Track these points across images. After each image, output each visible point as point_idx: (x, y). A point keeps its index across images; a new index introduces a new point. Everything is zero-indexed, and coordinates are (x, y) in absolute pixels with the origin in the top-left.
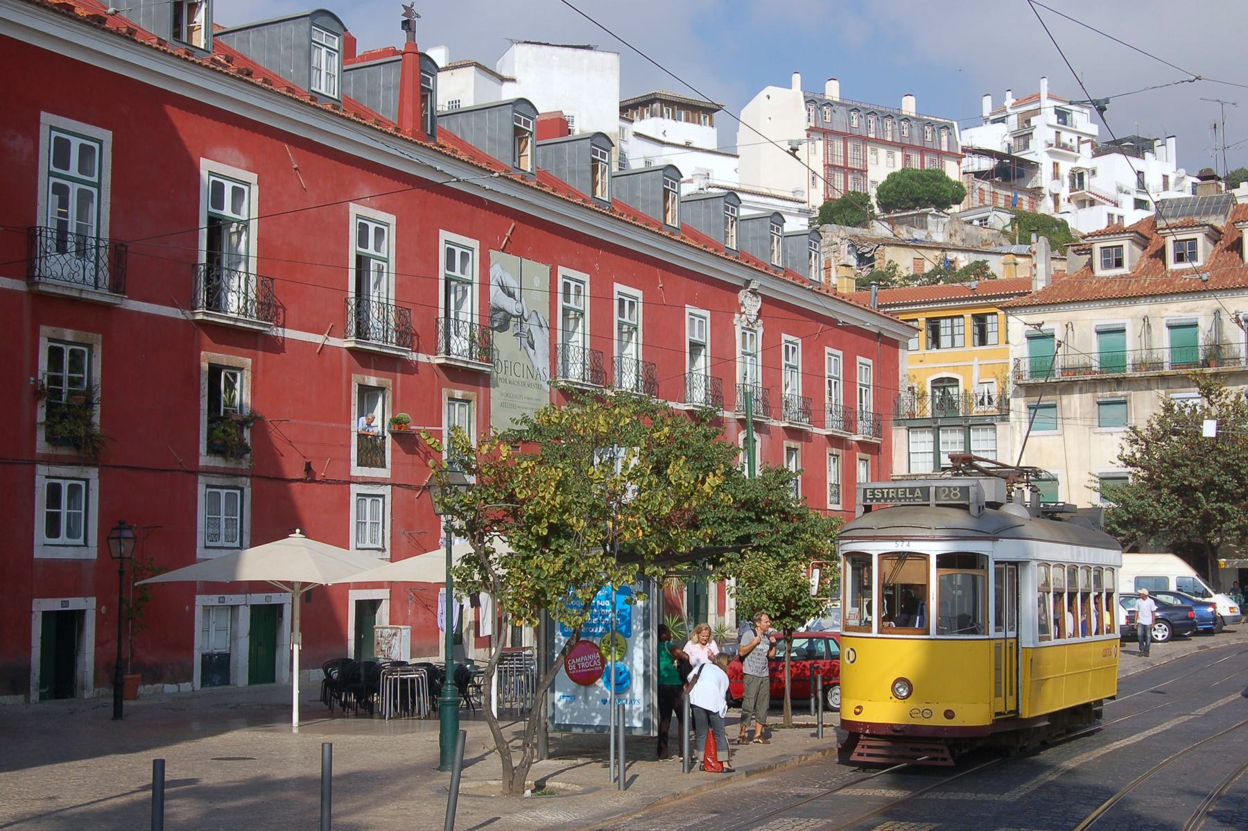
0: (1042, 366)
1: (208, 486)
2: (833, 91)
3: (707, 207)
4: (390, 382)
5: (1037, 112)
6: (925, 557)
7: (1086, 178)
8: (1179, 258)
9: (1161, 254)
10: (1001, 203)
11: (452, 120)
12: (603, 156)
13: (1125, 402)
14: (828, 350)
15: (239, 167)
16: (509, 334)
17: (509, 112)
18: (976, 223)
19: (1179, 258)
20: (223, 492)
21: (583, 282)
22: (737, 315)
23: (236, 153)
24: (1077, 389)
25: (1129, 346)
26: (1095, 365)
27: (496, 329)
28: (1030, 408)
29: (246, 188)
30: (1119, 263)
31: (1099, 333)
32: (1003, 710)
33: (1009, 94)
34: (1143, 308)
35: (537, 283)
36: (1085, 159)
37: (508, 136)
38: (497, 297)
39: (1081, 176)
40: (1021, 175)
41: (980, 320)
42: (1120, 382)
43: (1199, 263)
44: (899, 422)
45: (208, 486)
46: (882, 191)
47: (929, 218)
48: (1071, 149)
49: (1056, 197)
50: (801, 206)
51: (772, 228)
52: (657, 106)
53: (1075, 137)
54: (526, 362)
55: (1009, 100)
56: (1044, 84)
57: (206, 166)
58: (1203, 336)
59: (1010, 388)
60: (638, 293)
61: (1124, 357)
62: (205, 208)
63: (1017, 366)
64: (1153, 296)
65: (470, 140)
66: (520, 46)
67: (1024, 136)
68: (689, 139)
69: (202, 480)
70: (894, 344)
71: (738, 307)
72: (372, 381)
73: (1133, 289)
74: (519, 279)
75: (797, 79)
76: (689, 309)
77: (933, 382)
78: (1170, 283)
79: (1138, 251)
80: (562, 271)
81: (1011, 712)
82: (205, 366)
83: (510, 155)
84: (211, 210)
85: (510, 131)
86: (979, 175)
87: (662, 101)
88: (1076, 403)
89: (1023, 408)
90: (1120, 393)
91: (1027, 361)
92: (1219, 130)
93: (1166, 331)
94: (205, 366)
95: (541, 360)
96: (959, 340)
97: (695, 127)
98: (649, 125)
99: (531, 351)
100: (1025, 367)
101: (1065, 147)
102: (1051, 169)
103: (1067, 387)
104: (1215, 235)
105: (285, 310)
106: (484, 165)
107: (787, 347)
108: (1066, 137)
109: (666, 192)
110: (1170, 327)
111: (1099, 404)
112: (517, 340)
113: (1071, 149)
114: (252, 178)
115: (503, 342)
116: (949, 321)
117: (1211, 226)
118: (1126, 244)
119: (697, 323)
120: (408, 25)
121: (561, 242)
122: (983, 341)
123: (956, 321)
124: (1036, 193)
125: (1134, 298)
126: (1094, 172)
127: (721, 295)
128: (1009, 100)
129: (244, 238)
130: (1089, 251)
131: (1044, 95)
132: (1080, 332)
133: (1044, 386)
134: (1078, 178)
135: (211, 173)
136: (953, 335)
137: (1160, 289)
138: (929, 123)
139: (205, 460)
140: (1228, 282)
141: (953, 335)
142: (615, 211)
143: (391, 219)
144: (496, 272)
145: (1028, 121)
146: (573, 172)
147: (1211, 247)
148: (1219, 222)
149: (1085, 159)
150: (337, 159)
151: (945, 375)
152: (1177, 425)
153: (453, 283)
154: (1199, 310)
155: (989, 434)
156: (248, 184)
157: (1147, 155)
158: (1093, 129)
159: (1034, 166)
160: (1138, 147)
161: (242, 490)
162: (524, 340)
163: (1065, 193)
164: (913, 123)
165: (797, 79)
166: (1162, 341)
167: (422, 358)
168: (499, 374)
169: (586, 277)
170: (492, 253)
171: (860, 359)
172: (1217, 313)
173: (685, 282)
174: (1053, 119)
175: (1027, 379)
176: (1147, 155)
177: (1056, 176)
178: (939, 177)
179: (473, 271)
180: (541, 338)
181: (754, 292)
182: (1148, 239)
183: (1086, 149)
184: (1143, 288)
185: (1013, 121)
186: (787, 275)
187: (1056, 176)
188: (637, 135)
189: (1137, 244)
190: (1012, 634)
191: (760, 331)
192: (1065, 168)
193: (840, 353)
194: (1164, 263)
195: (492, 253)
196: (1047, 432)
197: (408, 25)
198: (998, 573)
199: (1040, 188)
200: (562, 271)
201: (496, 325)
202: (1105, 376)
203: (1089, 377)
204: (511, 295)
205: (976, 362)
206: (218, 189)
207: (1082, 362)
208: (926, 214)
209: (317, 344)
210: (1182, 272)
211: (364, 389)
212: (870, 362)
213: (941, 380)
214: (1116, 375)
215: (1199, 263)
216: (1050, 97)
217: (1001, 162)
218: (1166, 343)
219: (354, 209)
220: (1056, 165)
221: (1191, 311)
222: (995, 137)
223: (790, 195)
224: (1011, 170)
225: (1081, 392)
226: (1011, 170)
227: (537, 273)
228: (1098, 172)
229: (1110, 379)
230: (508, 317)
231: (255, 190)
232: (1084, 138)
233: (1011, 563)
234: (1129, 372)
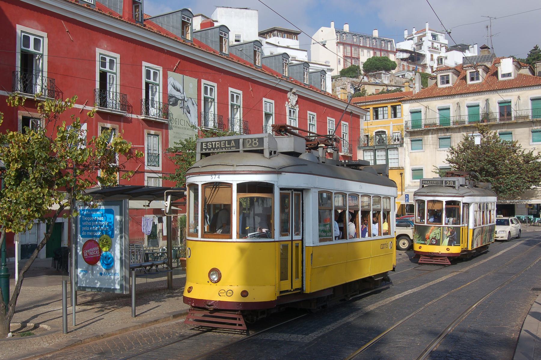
0: (416, 123)
2: (346, 28)
3: (275, 59)
4: (118, 126)
5: (424, 35)
6: (229, 185)
7: (443, 60)
8: (472, 79)
9: (465, 78)
11: (157, 19)
12: (225, 35)
13: (450, 138)
14: (328, 118)
15: (37, 29)
16: (177, 107)
17: (179, 14)
18: (401, 76)
19: (472, 79)
22: (287, 102)
23: (36, 23)
24: (430, 133)
25: (451, 115)
26: (438, 122)
27: (171, 105)
28: (412, 141)
29: (41, 39)
30: (448, 82)
31: (439, 110)
32: (289, 288)
33: (414, 29)
34: (457, 99)
35: (191, 85)
36: (443, 53)
37: (179, 25)
38: (171, 90)
39: (441, 59)
40: (419, 59)
41: (394, 108)
42: (448, 130)
43: (480, 81)
44: (360, 148)
46: (365, 65)
47: (382, 75)
48: (438, 49)
50: (328, 67)
51: (304, 68)
52: (276, 32)
53: (439, 45)
54: (186, 119)
55: (414, 31)
56: (427, 25)
57: (19, 28)
58: (481, 111)
59: (404, 133)
60: (240, 92)
61: (449, 120)
62: (19, 46)
63: (406, 124)
64: (461, 94)
65: (165, 27)
66: (219, 8)
67: (420, 45)
68: (288, 45)
70: (358, 117)
71: (287, 99)
73: (453, 92)
74: (182, 84)
75: (332, 24)
77: (376, 133)
78: (468, 89)
79: (455, 77)
80: (203, 81)
81: (296, 289)
82: (20, 117)
83: (180, 32)
84: (23, 48)
85: (180, 22)
86: (402, 59)
87: (277, 30)
88: (430, 139)
89: (409, 142)
90: (448, 134)
91: (410, 122)
92: (489, 28)
93: (466, 108)
94: (20, 117)
95: (193, 119)
96: (386, 116)
97: (290, 40)
98: (273, 40)
99: (188, 115)
100: (410, 124)
101: (435, 48)
102: (430, 57)
103: (427, 132)
104: (487, 70)
105: (62, 93)
106: (168, 36)
107: (310, 116)
108: (435, 45)
109: (255, 51)
110: (468, 107)
111: (440, 139)
113: (438, 49)
114: (45, 35)
116: (382, 109)
117: (485, 66)
118: (450, 74)
119: (268, 105)
121: (203, 69)
122: (395, 116)
123: (384, 108)
124: (424, 66)
126: (446, 58)
127: (280, 94)
128: (414, 31)
129: (41, 61)
130: (436, 78)
132: (431, 110)
133: (417, 132)
134: (440, 60)
135: (22, 32)
136: (383, 114)
138: (384, 40)
140: (491, 89)
141: (383, 114)
142: (230, 58)
143: (118, 56)
144: (171, 80)
145: (421, 39)
146: (212, 42)
147: (485, 75)
148: (489, 65)
149: (443, 53)
150: (83, 27)
151: (380, 130)
152: (468, 145)
153: (150, 85)
154: (479, 100)
155: (396, 152)
156: (43, 37)
157: (467, 51)
158: (446, 42)
159: (423, 56)
160: (463, 48)
162: (185, 110)
163: (435, 66)
164: (377, 40)
165: (332, 24)
166: (465, 112)
167: (134, 116)
168: (172, 124)
169: (215, 85)
170: (169, 72)
171: (342, 122)
172: (487, 100)
173: (262, 88)
174: (431, 38)
175: (410, 129)
177: (432, 59)
178: (387, 59)
179: (160, 79)
180: (194, 110)
181: (294, 93)
182: (460, 72)
183: (443, 49)
184: (457, 91)
185: (416, 39)
186: (310, 88)
187: (432, 59)
188: (267, 43)
189: (455, 74)
190: (300, 237)
191: (297, 110)
192: (436, 56)
193: (334, 120)
194: (466, 82)
195: (169, 72)
196: (419, 151)
198: (284, 198)
199: (426, 64)
200: (203, 81)
201: (171, 103)
202: (441, 127)
203: (435, 128)
204: (178, 90)
205: (391, 124)
206: (26, 39)
207: (432, 122)
208: (381, 73)
209: (79, 109)
210: (473, 85)
212: (347, 124)
213: (379, 132)
214: (446, 127)
215: (480, 81)
216: (429, 30)
217: (411, 55)
219: (98, 51)
220: (432, 55)
221: (477, 100)
222: (409, 45)
223: (324, 64)
224: (415, 58)
225: (432, 134)
226: (415, 58)
227: (191, 82)
228: (448, 58)
229: (444, 129)
230: (177, 100)
231: (46, 40)
232: (442, 45)
233: (296, 190)
234: (452, 125)
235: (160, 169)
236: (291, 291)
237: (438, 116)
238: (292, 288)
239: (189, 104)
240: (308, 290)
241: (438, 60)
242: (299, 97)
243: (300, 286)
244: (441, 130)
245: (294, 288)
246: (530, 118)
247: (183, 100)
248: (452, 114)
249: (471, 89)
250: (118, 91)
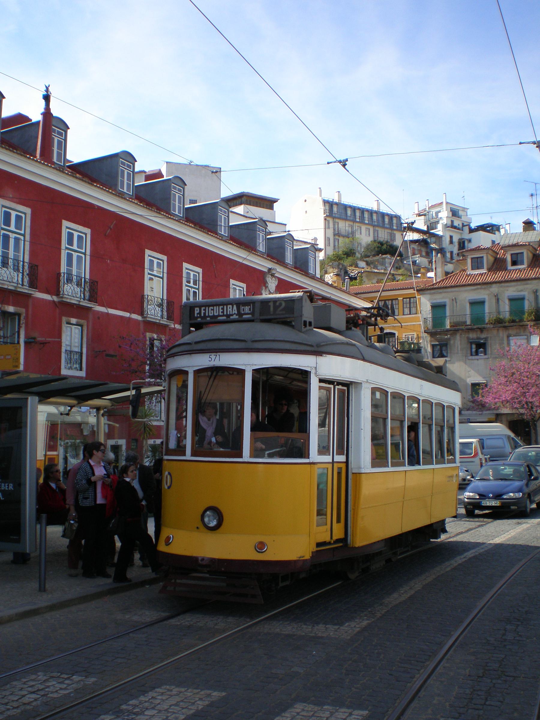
8: (514, 263)
10: (424, 254)
19: (514, 263)
21: (163, 261)
25: (487, 310)
32: (328, 539)
34: (495, 289)
39: (464, 242)
42: (482, 330)
48: (459, 229)
49: (452, 253)
61: (484, 319)
71: (265, 284)
73: (489, 279)
76: (232, 281)
81: (338, 541)
86: (413, 242)
101: (455, 227)
120: (47, 98)
126: (470, 241)
134: (462, 244)
166: (506, 308)
176: (497, 232)
177: (451, 242)
181: (273, 275)
183: (466, 229)
192: (456, 239)
197: (47, 98)
218: (507, 308)
220: (451, 237)
221: (521, 291)
228: (472, 241)
232: (465, 224)
236: (329, 543)
237: (468, 311)
238: (331, 538)
240: (360, 540)
241: (459, 243)
242: (281, 281)
243: (342, 536)
244: (472, 330)
245: (335, 538)
248: (488, 309)
249: (515, 276)
250: (27, 259)
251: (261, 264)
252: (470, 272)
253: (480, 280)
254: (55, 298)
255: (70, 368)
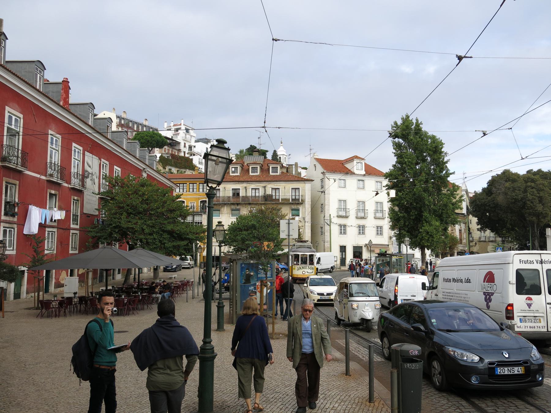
1: (4, 227)
5: (180, 129)
7: (193, 148)
9: (248, 170)
20: (8, 230)
23: (17, 106)
34: (245, 185)
36: (193, 143)
39: (191, 147)
42: (238, 204)
45: (4, 227)
49: (185, 152)
69: (2, 224)
72: (53, 192)
73: (241, 179)
74: (93, 163)
80: (102, 160)
112: (91, 182)
114: (21, 116)
115: (88, 182)
118: (239, 167)
124: (179, 150)
125: (243, 182)
126: (195, 147)
131: (182, 124)
134: (190, 148)
137: (249, 180)
139: (3, 218)
154: (260, 186)
156: (20, 118)
158: (195, 135)
159: (179, 143)
161: (14, 229)
163: (187, 151)
177: (185, 146)
180: (97, 181)
187: (185, 146)
200: (102, 160)
204: (90, 167)
210: (253, 176)
211: (51, 195)
215: (258, 174)
220: (185, 144)
231: (22, 120)
235: (78, 227)
239: (94, 177)
244: (233, 204)
246: (291, 201)
247: (92, 174)
249: (253, 179)
251: (141, 166)
252: (231, 174)
253: (237, 179)
254: (70, 187)
255: (73, 224)
